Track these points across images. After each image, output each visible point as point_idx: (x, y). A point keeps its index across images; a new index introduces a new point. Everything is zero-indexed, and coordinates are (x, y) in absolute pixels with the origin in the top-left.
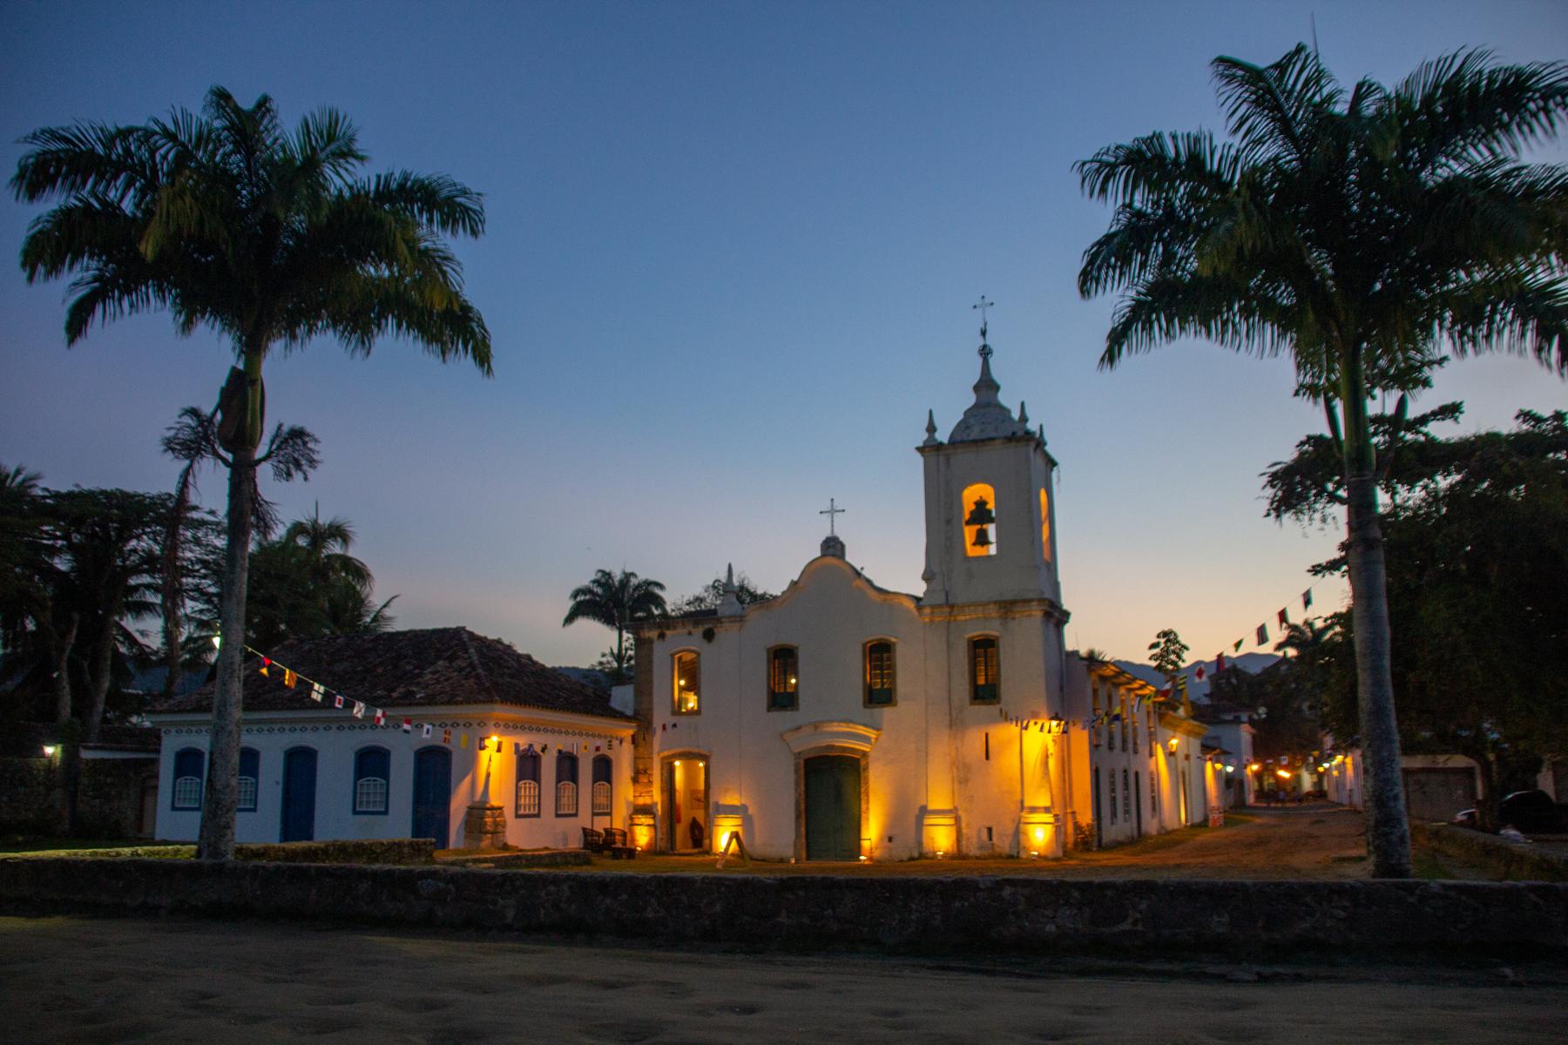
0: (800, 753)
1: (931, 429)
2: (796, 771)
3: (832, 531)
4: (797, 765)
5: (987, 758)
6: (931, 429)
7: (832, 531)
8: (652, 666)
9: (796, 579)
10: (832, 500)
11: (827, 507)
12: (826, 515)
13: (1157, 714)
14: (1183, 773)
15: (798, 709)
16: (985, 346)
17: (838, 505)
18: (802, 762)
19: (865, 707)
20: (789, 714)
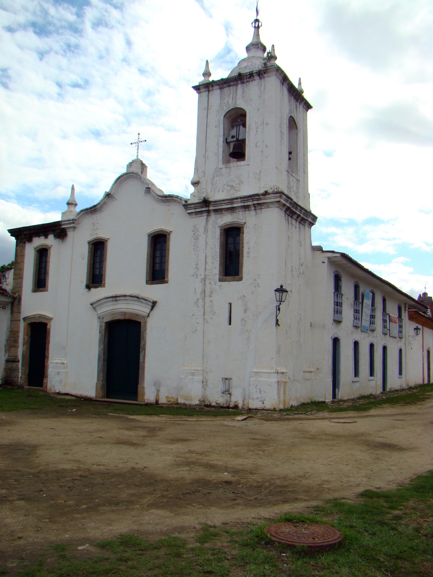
0: (103, 318)
1: (207, 74)
2: (100, 332)
3: (138, 156)
4: (101, 326)
5: (230, 324)
6: (207, 74)
7: (138, 156)
8: (24, 258)
9: (108, 190)
10: (139, 134)
11: (134, 139)
12: (135, 145)
13: (407, 312)
14: (428, 352)
15: (104, 286)
16: (257, 21)
17: (142, 138)
18: (104, 324)
19: (147, 283)
20: (99, 289)
